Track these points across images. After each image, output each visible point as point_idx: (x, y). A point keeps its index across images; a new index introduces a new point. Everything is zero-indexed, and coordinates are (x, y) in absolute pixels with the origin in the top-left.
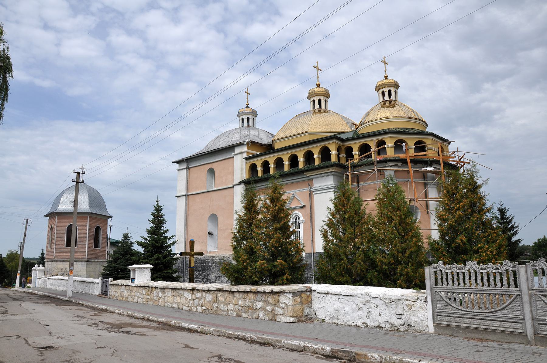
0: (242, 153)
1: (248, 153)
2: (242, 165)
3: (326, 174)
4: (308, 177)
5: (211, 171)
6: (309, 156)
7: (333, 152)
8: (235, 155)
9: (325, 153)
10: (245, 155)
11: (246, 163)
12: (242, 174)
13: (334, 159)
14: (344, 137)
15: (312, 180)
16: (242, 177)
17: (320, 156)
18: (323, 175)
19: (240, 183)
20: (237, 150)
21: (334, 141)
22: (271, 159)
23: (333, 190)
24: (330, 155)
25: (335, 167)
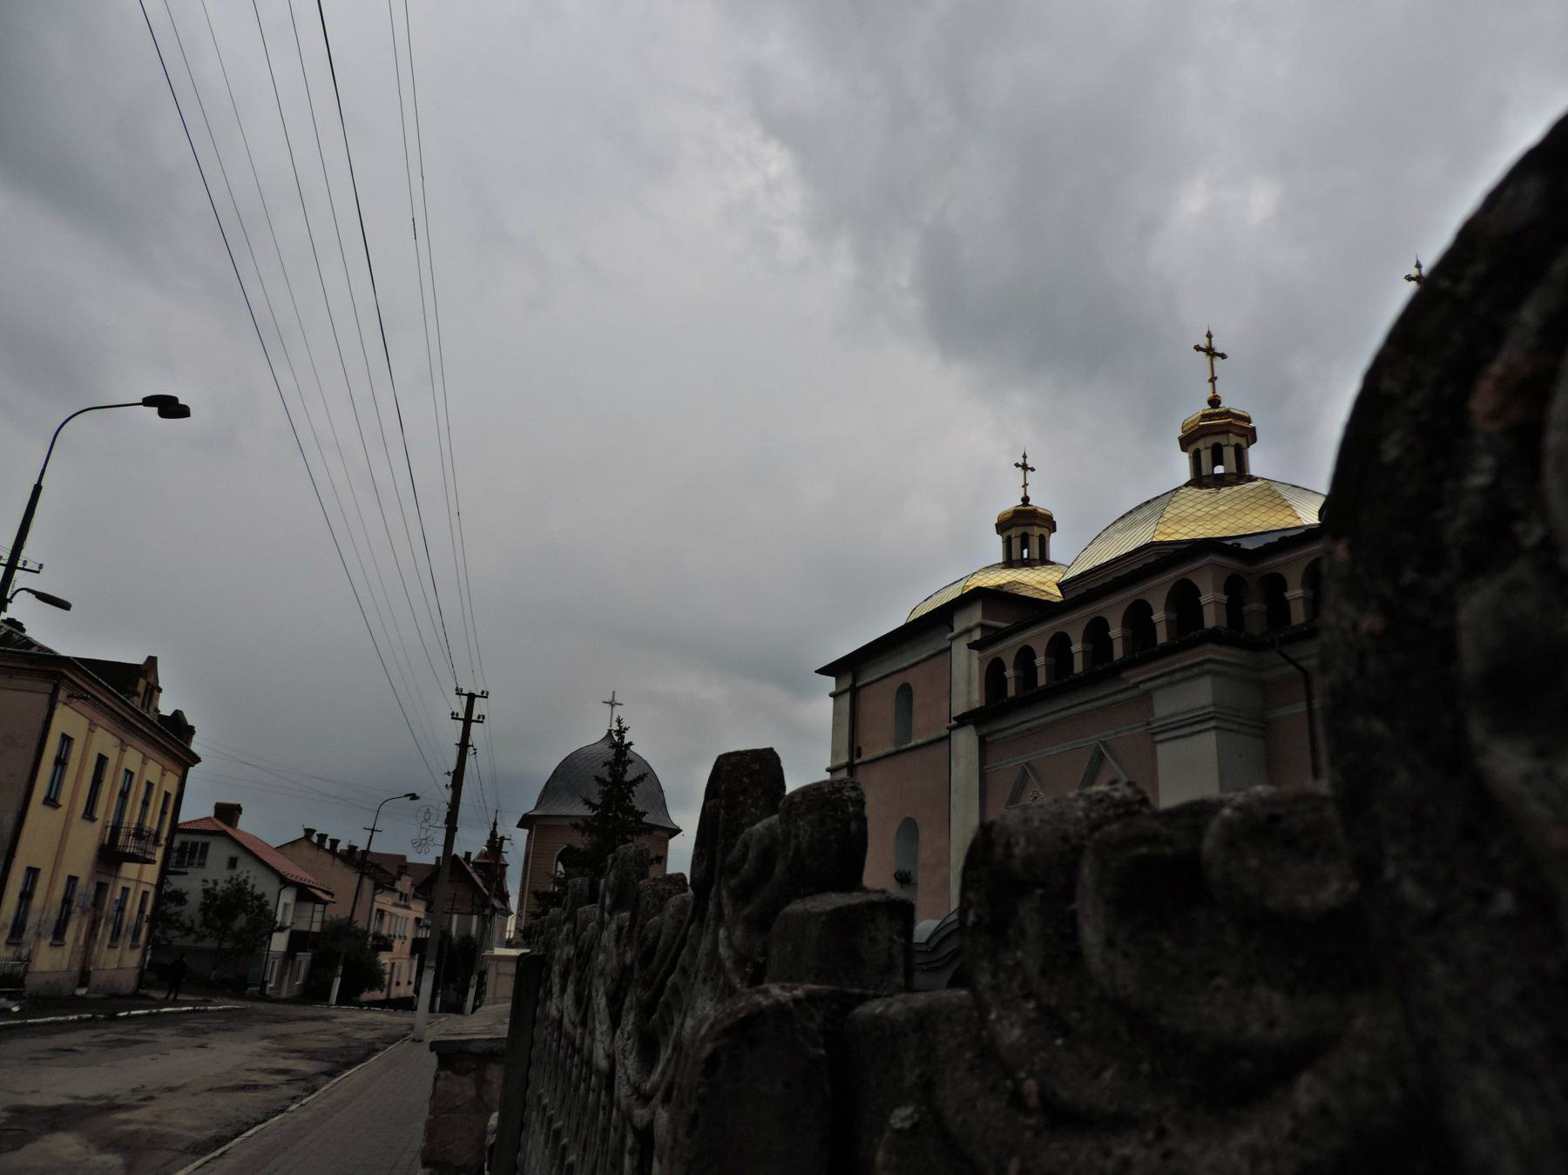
0: (969, 631)
1: (983, 626)
2: (970, 667)
3: (1188, 673)
4: (1136, 685)
5: (905, 692)
6: (1138, 615)
7: (1210, 598)
8: (952, 640)
9: (1185, 600)
10: (977, 635)
11: (981, 660)
12: (969, 693)
13: (1210, 619)
14: (1248, 545)
15: (1148, 695)
16: (969, 702)
17: (1174, 616)
18: (1178, 676)
19: (962, 721)
20: (960, 623)
21: (1213, 558)
22: (1038, 638)
23: (1212, 724)
24: (1201, 607)
25: (1210, 646)
